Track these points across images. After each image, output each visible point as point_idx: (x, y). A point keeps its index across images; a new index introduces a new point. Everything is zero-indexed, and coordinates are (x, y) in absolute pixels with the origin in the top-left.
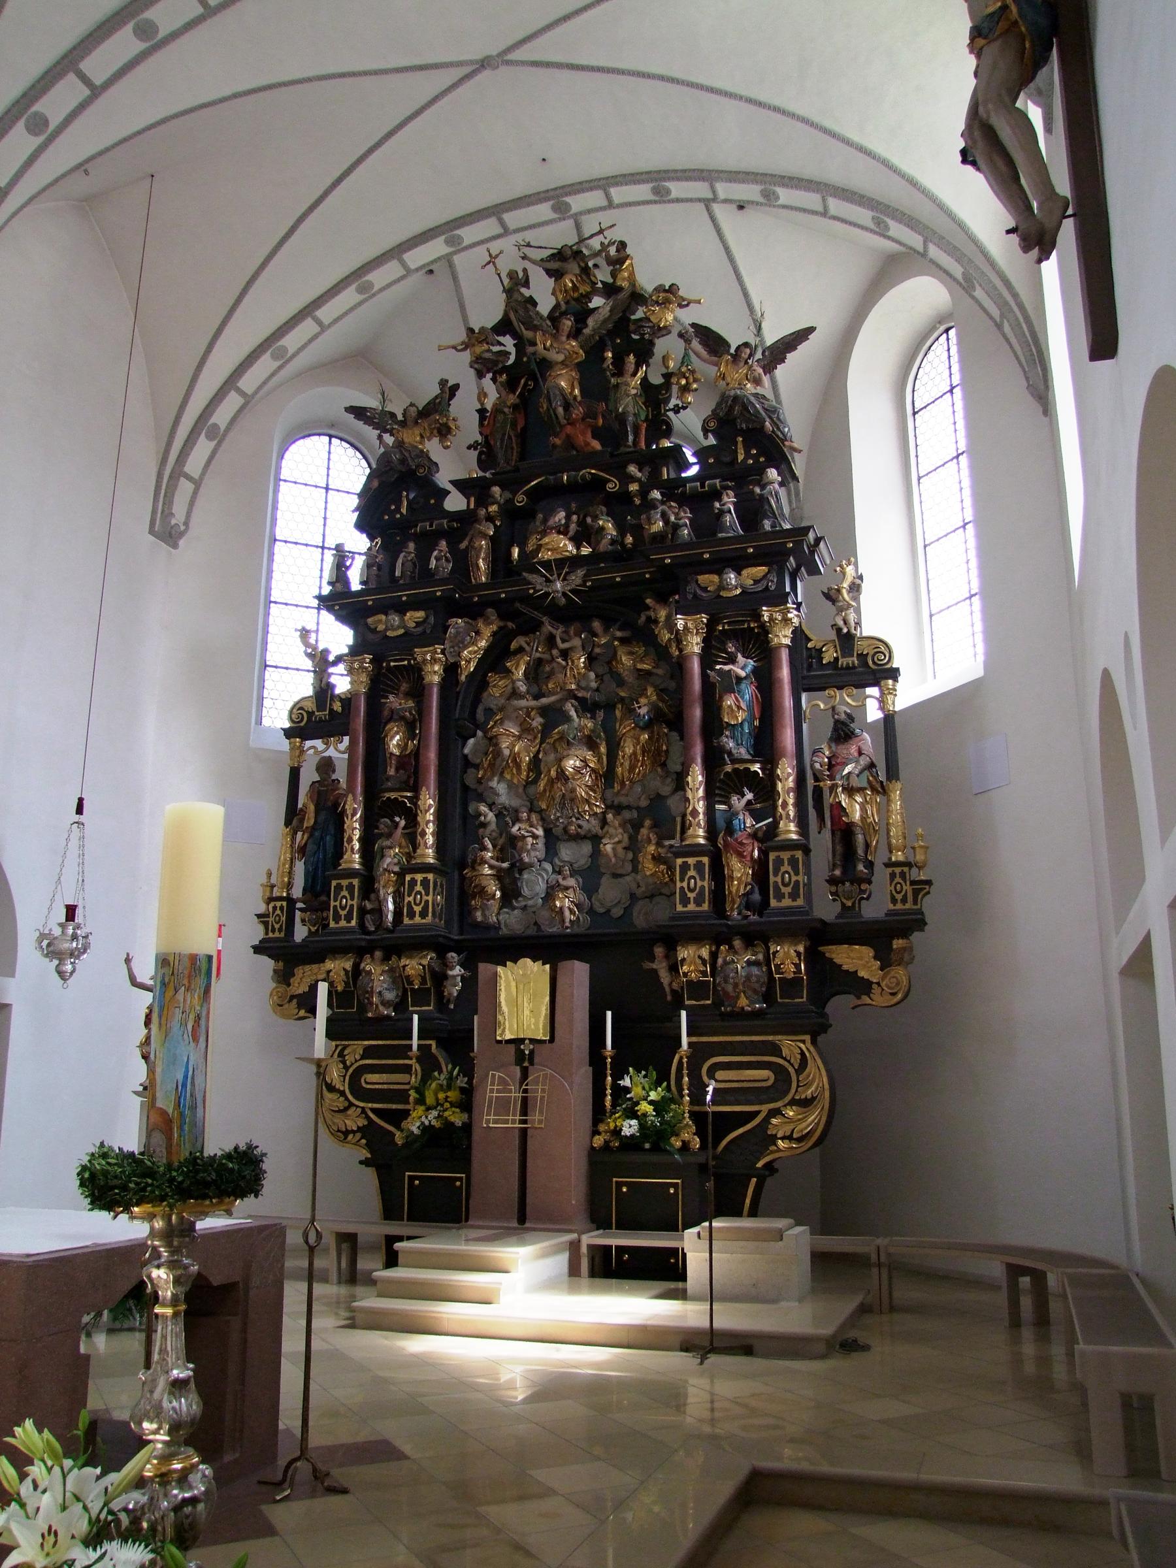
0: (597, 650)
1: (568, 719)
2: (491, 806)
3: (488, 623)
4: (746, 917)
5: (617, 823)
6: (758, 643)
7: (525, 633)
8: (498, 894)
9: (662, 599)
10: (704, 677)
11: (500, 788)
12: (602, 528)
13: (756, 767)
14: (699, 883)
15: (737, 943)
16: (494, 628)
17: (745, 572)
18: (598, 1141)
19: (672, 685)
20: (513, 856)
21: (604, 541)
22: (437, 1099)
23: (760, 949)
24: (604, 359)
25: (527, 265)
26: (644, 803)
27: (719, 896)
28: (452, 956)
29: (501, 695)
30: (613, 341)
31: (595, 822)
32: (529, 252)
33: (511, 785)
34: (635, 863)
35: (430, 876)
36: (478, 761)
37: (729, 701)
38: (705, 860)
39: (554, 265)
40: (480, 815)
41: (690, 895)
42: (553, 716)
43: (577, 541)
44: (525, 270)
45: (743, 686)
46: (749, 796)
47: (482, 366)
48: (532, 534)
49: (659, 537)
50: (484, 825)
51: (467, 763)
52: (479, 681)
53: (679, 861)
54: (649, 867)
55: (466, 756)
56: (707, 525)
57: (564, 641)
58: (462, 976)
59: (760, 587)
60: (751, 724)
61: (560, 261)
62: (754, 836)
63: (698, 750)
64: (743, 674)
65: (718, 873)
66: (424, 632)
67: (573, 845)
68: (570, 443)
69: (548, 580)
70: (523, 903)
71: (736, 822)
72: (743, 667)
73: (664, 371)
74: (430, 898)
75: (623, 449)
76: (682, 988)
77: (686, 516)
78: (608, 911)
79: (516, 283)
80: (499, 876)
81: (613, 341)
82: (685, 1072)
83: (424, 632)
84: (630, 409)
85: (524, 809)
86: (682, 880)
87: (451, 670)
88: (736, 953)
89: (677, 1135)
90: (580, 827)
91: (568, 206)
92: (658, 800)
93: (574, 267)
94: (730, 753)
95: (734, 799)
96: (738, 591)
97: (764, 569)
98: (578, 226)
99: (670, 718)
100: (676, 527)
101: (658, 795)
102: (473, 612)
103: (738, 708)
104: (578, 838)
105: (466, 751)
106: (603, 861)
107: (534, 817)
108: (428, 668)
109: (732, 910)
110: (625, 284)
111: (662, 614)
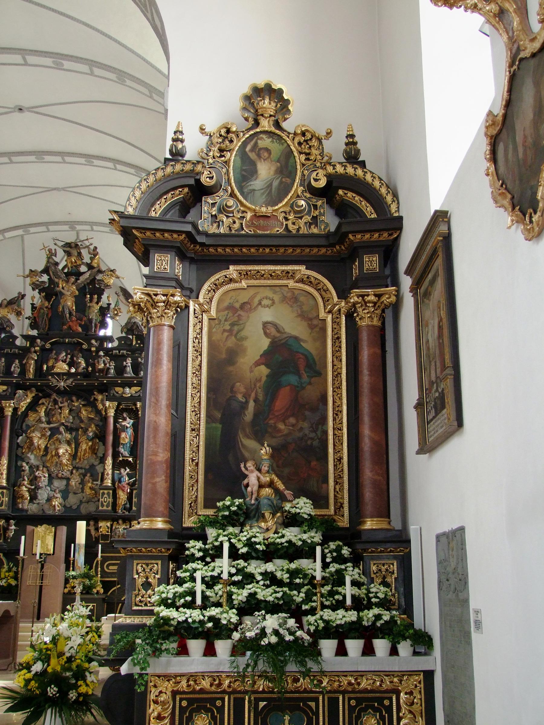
0: (74, 408)
1: (61, 433)
2: (27, 463)
3: (31, 392)
4: (124, 513)
5: (77, 474)
6: (134, 413)
7: (45, 397)
8: (29, 498)
9: (101, 392)
10: (115, 426)
11: (32, 458)
12: (80, 363)
13: (131, 459)
14: (108, 500)
15: (120, 522)
16: (33, 395)
17: (132, 388)
18: (66, 590)
19: (101, 424)
20: (36, 484)
21: (81, 368)
22: (5, 575)
23: (128, 524)
24: (86, 297)
25: (56, 247)
26: (87, 467)
27: (114, 504)
28: (12, 522)
29: (34, 420)
30: (89, 286)
31: (68, 473)
32: (57, 242)
33: (35, 456)
34: (83, 490)
35: (5, 491)
36: (22, 445)
37: (123, 435)
38: (111, 492)
39: (68, 249)
40: (23, 467)
41: (104, 503)
42: (55, 431)
43: (70, 365)
44: (55, 250)
45: (128, 430)
46: (128, 470)
47: (34, 286)
48: (51, 358)
49: (101, 371)
50: (24, 471)
51: (18, 446)
52: (25, 414)
53: (101, 491)
54: (88, 491)
55: (18, 443)
56: (120, 370)
57: (61, 403)
58: (15, 530)
59: (137, 395)
60: (130, 443)
61: (71, 248)
62: (128, 484)
63: (110, 452)
64: (129, 426)
65: (115, 496)
66: (6, 394)
67: (59, 480)
68: (70, 328)
69: (58, 381)
70: (38, 502)
71: (122, 479)
72: (128, 423)
73: (108, 302)
74: (4, 499)
75: (90, 333)
76: (99, 536)
77: (113, 364)
78: (71, 507)
79: (51, 254)
80: (29, 491)
81: (89, 286)
82: (99, 566)
83: (6, 394)
84: (94, 317)
85: (41, 466)
86: (102, 498)
87: (15, 410)
88: (119, 525)
89: (95, 588)
90: (63, 474)
91: (76, 228)
92: (92, 466)
93: (75, 252)
94: (122, 454)
95: (122, 470)
96: (130, 395)
97: (140, 388)
98: (78, 234)
99: (101, 436)
100: (108, 369)
101: (93, 465)
102: (26, 388)
103: (126, 437)
104: (61, 478)
105: (18, 441)
106: (70, 488)
107: (45, 469)
108: (6, 409)
109: (119, 509)
110: (95, 265)
111: (100, 397)
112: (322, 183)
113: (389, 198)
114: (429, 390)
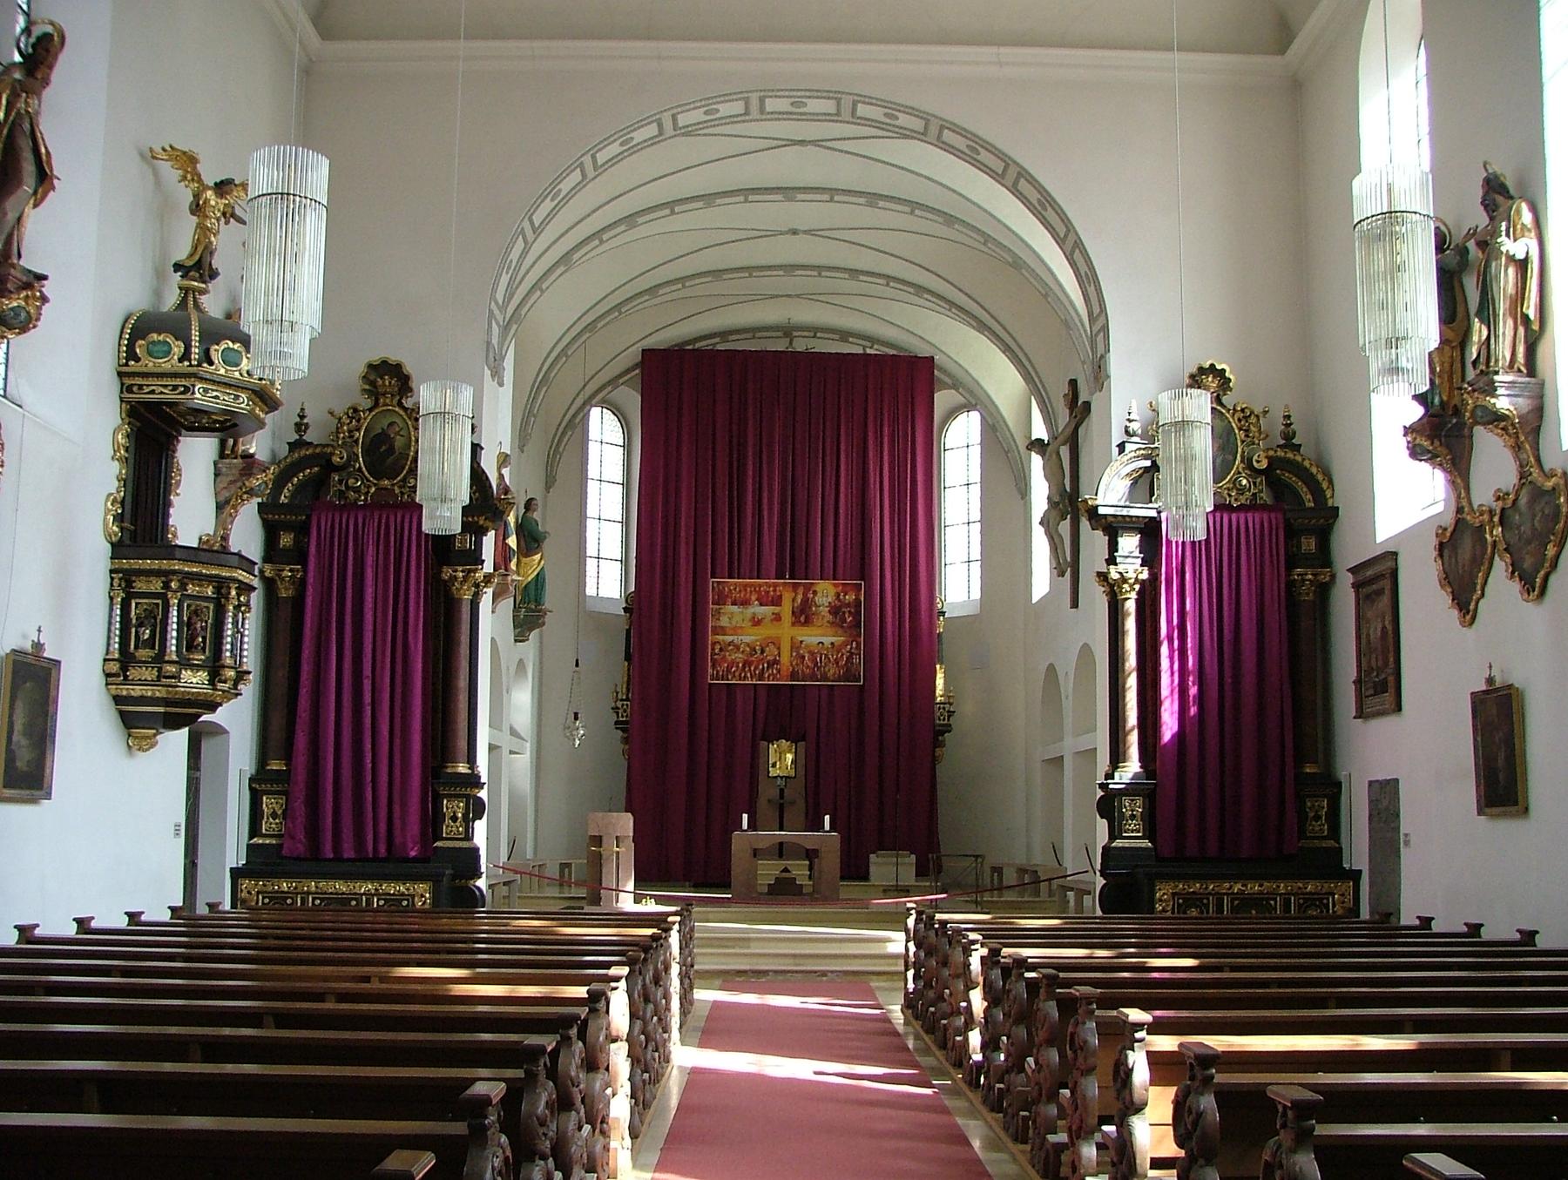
112: (1264, 464)
113: (1325, 485)
114: (1368, 673)
